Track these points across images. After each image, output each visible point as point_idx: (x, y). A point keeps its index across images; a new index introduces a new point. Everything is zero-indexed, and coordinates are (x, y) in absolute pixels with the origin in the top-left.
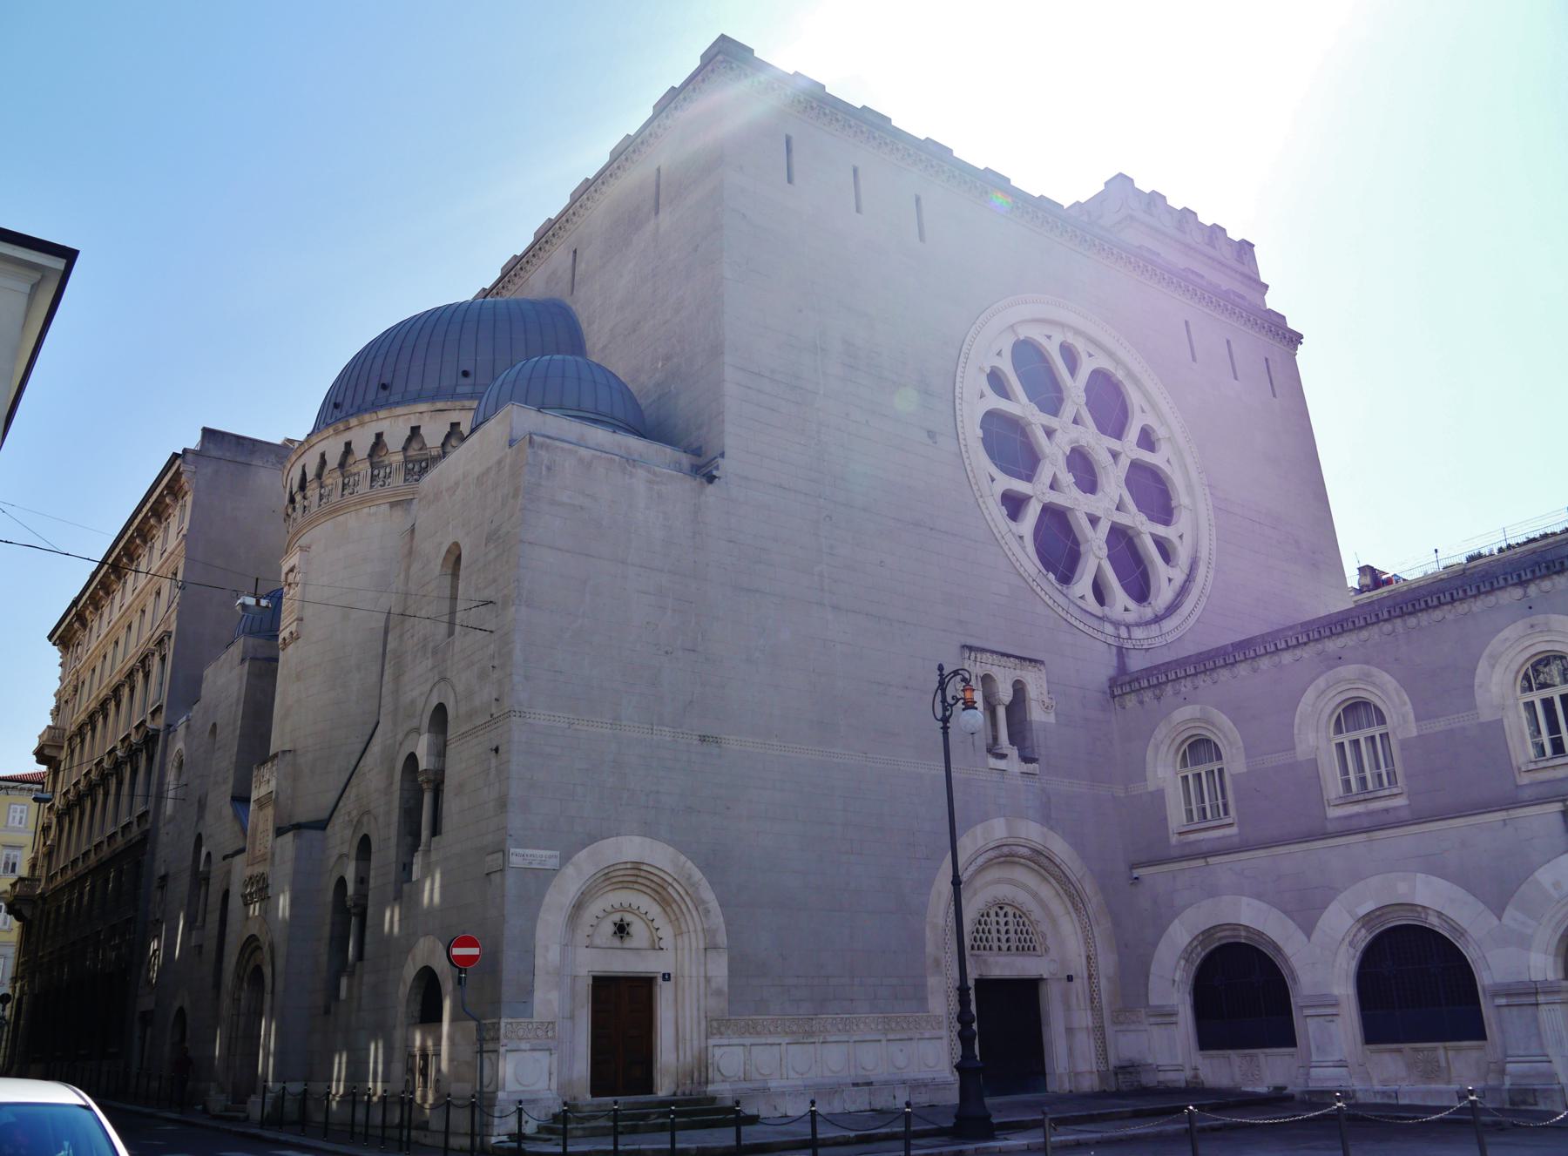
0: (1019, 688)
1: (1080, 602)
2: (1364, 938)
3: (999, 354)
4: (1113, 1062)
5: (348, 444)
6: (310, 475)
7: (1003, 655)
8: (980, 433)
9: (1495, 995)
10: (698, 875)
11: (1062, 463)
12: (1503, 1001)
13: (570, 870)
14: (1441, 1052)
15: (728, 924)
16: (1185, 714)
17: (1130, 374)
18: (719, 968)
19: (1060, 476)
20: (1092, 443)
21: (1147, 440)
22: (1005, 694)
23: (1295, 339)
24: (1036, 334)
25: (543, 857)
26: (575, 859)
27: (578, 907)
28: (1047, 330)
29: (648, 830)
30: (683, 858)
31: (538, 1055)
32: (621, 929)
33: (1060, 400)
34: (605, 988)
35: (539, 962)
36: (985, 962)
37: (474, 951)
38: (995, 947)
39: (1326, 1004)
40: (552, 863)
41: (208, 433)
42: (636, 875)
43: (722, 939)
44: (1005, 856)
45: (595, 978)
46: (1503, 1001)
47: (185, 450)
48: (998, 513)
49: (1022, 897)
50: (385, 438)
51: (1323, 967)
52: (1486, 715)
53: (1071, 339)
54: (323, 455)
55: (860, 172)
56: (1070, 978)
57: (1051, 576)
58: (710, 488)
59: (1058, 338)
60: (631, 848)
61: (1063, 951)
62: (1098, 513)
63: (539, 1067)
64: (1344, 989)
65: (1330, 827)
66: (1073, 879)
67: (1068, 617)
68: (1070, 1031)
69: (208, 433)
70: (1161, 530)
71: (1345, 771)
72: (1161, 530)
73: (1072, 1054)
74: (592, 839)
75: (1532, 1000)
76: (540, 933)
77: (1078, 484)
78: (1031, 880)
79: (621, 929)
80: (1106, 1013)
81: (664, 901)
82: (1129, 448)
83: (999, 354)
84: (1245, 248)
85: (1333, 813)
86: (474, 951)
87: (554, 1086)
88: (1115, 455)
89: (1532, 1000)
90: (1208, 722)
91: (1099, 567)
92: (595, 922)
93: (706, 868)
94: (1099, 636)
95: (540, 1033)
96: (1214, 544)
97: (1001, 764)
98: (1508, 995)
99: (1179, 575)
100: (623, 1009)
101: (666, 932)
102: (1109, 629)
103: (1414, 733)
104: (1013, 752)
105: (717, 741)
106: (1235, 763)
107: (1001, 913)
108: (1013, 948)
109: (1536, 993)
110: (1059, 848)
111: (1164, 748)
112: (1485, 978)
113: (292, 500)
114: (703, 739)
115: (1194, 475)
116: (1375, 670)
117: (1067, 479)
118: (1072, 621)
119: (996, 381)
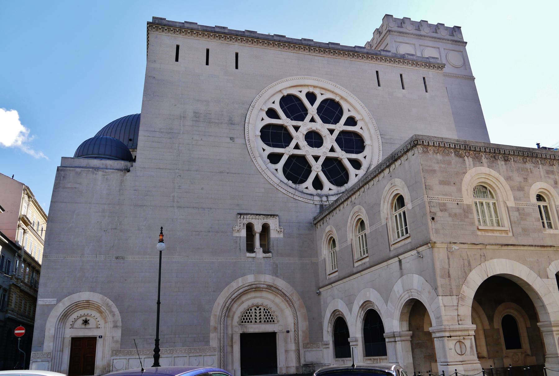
1: (305, 191)
2: (363, 314)
3: (274, 103)
4: (303, 362)
7: (257, 215)
8: (260, 134)
10: (111, 303)
13: (60, 304)
15: (122, 319)
17: (342, 98)
18: (118, 334)
19: (299, 143)
22: (258, 228)
25: (52, 301)
26: (63, 300)
29: (92, 289)
30: (106, 298)
31: (44, 363)
32: (86, 322)
33: (307, 114)
34: (76, 342)
35: (47, 334)
36: (246, 327)
38: (253, 321)
43: (120, 324)
45: (72, 338)
48: (262, 163)
49: (266, 303)
53: (311, 90)
56: (288, 332)
57: (290, 182)
58: (128, 174)
59: (305, 90)
60: (85, 296)
61: (286, 321)
65: (355, 270)
66: (288, 295)
67: (295, 197)
68: (287, 351)
70: (353, 156)
72: (353, 156)
74: (70, 294)
76: (48, 325)
78: (271, 296)
79: (86, 322)
80: (301, 344)
81: (101, 312)
83: (274, 103)
85: (356, 265)
88: (332, 131)
93: (115, 300)
94: (311, 202)
95: (45, 356)
97: (253, 255)
101: (102, 322)
102: (317, 198)
105: (123, 258)
107: (258, 309)
108: (263, 321)
109: (394, 337)
110: (281, 283)
111: (325, 242)
115: (373, 131)
117: (303, 143)
119: (272, 113)
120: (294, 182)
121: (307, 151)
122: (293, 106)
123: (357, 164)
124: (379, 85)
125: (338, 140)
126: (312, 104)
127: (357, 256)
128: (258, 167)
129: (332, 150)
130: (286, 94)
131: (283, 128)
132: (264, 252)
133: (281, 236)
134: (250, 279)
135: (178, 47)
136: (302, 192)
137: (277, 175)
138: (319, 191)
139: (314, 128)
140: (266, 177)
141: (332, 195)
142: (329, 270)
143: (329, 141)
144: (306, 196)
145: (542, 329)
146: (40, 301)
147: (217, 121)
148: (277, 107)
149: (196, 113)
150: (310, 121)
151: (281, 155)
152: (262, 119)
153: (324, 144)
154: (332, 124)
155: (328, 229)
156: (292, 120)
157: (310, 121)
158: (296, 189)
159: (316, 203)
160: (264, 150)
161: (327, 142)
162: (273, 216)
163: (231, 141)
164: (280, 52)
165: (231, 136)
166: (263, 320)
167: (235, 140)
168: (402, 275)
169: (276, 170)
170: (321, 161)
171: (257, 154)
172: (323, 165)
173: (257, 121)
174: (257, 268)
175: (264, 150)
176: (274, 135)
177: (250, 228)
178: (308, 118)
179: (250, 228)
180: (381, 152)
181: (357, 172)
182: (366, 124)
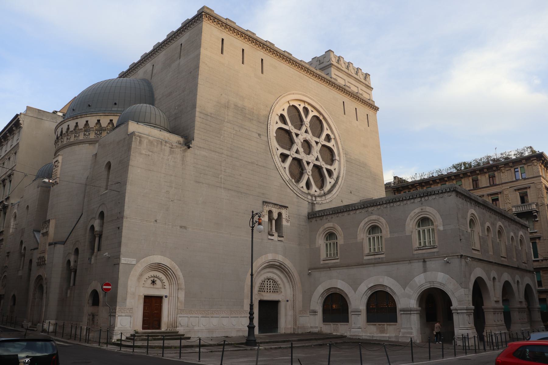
0: (280, 214)
1: (301, 189)
2: (370, 293)
3: (283, 110)
5: (77, 123)
6: (64, 132)
8: (275, 135)
9: (401, 311)
10: (177, 267)
11: (300, 144)
12: (402, 313)
13: (139, 265)
14: (386, 326)
16: (328, 224)
17: (324, 118)
18: (182, 295)
21: (328, 138)
22: (275, 216)
23: (376, 109)
24: (296, 104)
27: (141, 275)
28: (299, 103)
29: (163, 254)
32: (153, 282)
33: (302, 125)
35: (129, 290)
36: (262, 295)
37: (110, 287)
38: (266, 291)
39: (357, 312)
40: (134, 262)
41: (28, 108)
42: (159, 267)
44: (271, 266)
45: (145, 296)
46: (402, 313)
47: (21, 114)
48: (278, 160)
50: (89, 122)
51: (358, 301)
52: (408, 234)
53: (307, 106)
54: (68, 126)
55: (245, 51)
56: (287, 301)
57: (293, 180)
59: (303, 105)
62: (310, 161)
63: (128, 321)
64: (363, 307)
65: (364, 262)
68: (286, 315)
69: (28, 108)
70: (329, 167)
71: (370, 246)
73: (285, 323)
75: (409, 312)
76: (129, 283)
77: (305, 152)
79: (153, 282)
81: (166, 275)
83: (283, 110)
84: (367, 76)
85: (366, 258)
86: (110, 287)
87: (131, 326)
88: (317, 143)
89: (409, 312)
90: (334, 228)
91: (309, 178)
92: (146, 280)
94: (306, 199)
98: (404, 311)
99: (333, 182)
100: (153, 306)
101: (167, 283)
102: (309, 197)
103: (389, 236)
104: (276, 235)
106: (341, 241)
110: (288, 263)
112: (399, 306)
113: (58, 138)
114: (181, 227)
116: (381, 218)
117: (301, 150)
118: (298, 194)
123: (330, 172)
127: (367, 251)
131: (288, 132)
132: (279, 236)
133: (289, 224)
134: (270, 257)
135: (223, 40)
142: (323, 255)
145: (484, 310)
146: (123, 260)
147: (250, 117)
148: (285, 114)
149: (236, 106)
155: (330, 225)
162: (286, 207)
163: (258, 137)
165: (259, 132)
166: (271, 291)
167: (262, 136)
168: (425, 271)
170: (311, 165)
174: (273, 250)
177: (270, 212)
179: (270, 212)
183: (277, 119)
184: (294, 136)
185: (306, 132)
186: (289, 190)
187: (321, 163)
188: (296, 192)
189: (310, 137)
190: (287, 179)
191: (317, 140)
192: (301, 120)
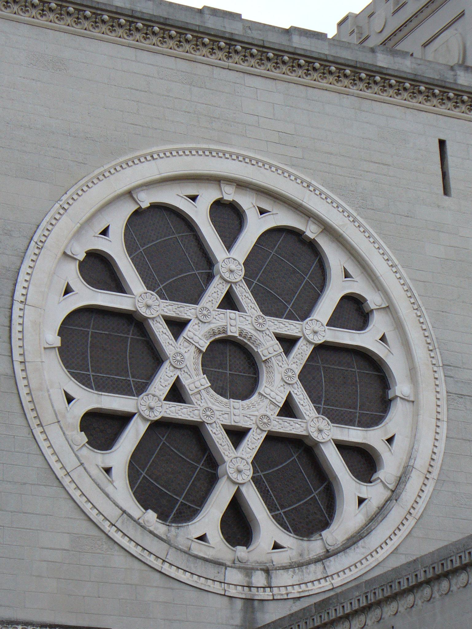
3: (105, 232)
8: (57, 341)
17: (327, 229)
19: (186, 382)
20: (248, 328)
21: (354, 311)
24: (174, 197)
33: (210, 277)
48: (65, 442)
53: (230, 194)
57: (151, 515)
59: (208, 196)
67: (166, 568)
70: (355, 435)
82: (318, 327)
83: (105, 232)
88: (288, 343)
94: (217, 588)
96: (442, 445)
102: (234, 576)
115: (420, 353)
117: (196, 381)
118: (172, 572)
120: (163, 517)
121: (210, 408)
122: (167, 244)
123: (363, 461)
124: (446, 191)
125: (307, 376)
126: (229, 242)
128: (52, 460)
129: (288, 410)
130: (145, 205)
131: (134, 321)
136: (187, 553)
137: (109, 489)
138: (241, 551)
139: (233, 332)
140: (76, 494)
141: (284, 568)
143: (281, 377)
144: (200, 568)
148: (115, 248)
150: (222, 306)
151: (124, 419)
152: (68, 290)
153: (264, 387)
154: (291, 317)
156: (162, 297)
157: (222, 306)
158: (166, 541)
159: (232, 591)
160: (70, 399)
161: (271, 383)
164: (130, 52)
169: (108, 470)
170: (253, 443)
171: (47, 417)
172: (259, 461)
173: (51, 295)
175: (70, 399)
176: (106, 346)
178: (215, 292)
180: (444, 426)
181: (364, 490)
182: (399, 325)
183: (71, 274)
184: (162, 333)
185: (229, 302)
186: (119, 560)
187: (312, 423)
188: (157, 564)
189: (251, 323)
190: (113, 513)
191: (289, 328)
192: (209, 261)
